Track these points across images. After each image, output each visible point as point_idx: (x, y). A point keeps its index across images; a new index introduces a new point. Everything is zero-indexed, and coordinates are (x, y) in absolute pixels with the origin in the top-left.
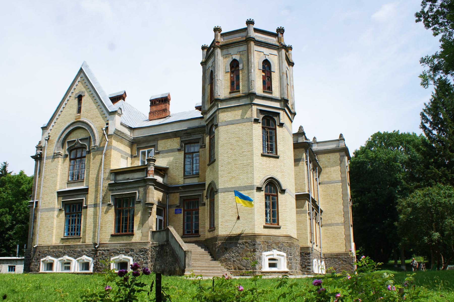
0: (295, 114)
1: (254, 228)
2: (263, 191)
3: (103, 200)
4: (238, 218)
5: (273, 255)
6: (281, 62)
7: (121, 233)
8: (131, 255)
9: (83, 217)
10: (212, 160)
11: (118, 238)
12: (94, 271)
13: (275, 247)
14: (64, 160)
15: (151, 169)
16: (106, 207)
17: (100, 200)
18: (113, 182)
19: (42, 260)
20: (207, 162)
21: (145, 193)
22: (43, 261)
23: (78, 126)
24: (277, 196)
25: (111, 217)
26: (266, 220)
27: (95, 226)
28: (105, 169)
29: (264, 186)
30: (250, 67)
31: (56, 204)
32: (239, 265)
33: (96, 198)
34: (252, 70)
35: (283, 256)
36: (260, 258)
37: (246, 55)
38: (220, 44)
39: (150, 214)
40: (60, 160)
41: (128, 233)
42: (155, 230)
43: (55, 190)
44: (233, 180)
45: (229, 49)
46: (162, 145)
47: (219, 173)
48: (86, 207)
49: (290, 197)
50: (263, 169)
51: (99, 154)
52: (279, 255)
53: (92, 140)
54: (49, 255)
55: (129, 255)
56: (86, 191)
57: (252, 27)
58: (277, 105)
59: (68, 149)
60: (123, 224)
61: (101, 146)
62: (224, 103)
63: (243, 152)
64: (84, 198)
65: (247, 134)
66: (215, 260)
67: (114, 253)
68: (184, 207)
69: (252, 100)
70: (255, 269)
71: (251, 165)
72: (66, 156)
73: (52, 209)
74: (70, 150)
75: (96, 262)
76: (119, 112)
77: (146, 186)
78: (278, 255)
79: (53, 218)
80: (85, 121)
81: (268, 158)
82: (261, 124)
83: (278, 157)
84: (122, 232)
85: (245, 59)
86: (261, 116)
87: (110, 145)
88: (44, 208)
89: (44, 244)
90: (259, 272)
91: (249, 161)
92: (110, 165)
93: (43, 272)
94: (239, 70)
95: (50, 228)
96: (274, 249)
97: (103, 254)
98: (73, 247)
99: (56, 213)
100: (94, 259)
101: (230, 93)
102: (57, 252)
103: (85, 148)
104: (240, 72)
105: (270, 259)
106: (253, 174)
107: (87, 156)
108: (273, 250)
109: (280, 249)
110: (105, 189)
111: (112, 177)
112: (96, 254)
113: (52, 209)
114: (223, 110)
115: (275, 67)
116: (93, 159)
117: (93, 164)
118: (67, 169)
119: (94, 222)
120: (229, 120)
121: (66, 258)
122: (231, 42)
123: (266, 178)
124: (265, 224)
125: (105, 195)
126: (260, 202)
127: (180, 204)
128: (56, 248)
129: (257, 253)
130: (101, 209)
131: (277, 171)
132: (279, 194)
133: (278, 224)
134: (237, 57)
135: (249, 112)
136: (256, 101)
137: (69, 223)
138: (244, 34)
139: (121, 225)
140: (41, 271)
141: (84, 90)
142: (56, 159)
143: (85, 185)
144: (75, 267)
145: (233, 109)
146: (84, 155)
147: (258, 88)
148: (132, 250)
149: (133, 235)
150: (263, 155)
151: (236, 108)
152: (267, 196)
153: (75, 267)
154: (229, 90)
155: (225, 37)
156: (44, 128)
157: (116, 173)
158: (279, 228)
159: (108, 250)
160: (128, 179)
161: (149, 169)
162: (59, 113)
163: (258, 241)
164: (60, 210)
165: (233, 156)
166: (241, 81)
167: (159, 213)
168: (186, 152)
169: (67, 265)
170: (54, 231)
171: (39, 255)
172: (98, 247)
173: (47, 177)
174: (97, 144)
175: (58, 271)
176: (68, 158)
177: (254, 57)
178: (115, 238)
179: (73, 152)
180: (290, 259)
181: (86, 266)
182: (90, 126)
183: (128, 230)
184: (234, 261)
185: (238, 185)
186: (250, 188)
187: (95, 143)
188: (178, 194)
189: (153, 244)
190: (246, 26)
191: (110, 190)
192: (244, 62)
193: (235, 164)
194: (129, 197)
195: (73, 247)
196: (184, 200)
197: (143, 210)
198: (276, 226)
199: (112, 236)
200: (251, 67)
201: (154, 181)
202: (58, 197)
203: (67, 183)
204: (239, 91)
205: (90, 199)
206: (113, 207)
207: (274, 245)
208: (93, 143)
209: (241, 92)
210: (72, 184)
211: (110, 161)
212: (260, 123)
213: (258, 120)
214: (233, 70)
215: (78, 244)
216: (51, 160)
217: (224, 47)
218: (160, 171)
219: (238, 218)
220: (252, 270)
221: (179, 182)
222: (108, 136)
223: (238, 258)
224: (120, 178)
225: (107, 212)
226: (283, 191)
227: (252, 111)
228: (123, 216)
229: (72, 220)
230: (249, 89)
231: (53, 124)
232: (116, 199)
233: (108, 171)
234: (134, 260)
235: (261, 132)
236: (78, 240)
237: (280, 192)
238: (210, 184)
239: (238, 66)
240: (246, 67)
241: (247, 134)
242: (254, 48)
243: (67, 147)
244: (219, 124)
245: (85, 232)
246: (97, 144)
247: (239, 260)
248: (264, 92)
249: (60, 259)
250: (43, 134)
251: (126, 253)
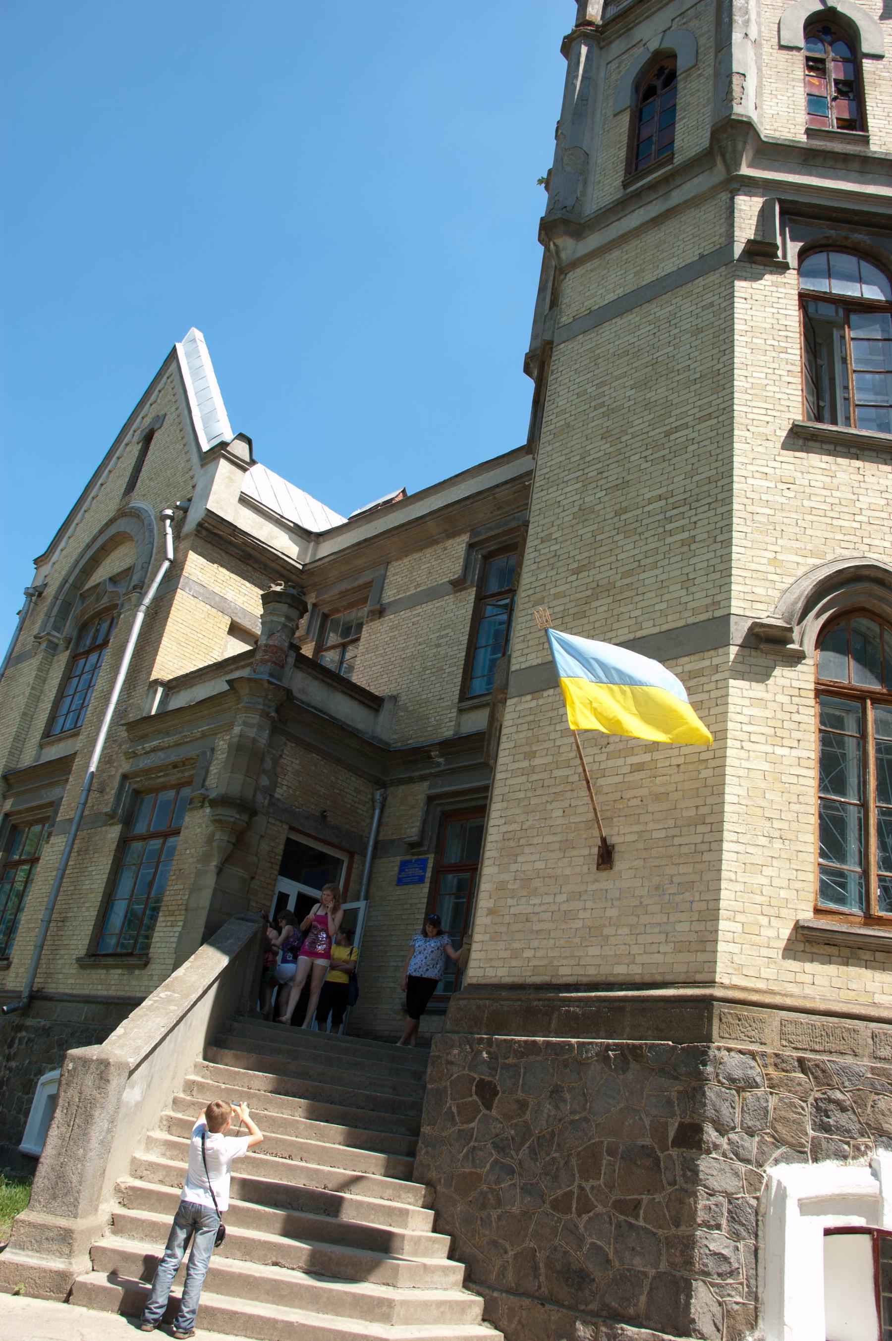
26: (832, 886)
29: (813, 625)
63: (667, 435)
65: (699, 330)
68: (440, 850)
120: (611, 297)
124: (806, 915)
126: (777, 739)
127: (423, 832)
163: (728, 1052)
188: (426, 784)
196: (447, 817)
241: (699, 330)
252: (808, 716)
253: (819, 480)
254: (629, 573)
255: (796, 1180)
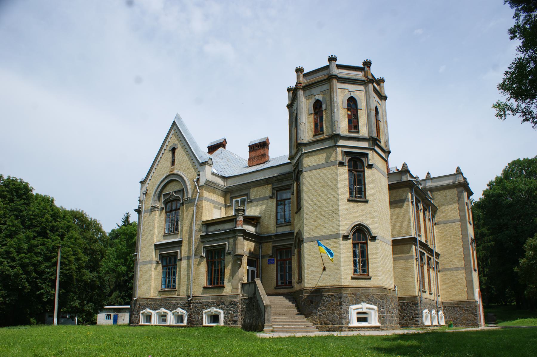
0: (389, 152)
1: (340, 280)
2: (350, 239)
3: (195, 252)
4: (324, 269)
5: (362, 308)
6: (368, 98)
7: (213, 286)
8: (222, 308)
9: (178, 269)
10: (299, 208)
11: (210, 290)
12: (188, 323)
13: (364, 300)
14: (161, 213)
15: (240, 219)
16: (199, 259)
17: (193, 252)
18: (205, 234)
19: (141, 312)
20: (296, 210)
21: (235, 244)
22: (142, 313)
23: (172, 179)
24: (367, 244)
25: (203, 269)
26: (355, 271)
27: (189, 279)
28: (197, 220)
29: (352, 234)
30: (333, 106)
31: (154, 257)
32: (325, 320)
33: (189, 250)
34: (335, 110)
35: (374, 309)
36: (347, 312)
37: (329, 94)
38: (303, 85)
39: (240, 265)
40: (157, 213)
41: (219, 285)
42: (245, 281)
43: (153, 243)
44: (319, 229)
45: (312, 90)
46: (254, 193)
47: (305, 221)
48: (181, 260)
49: (383, 243)
50: (349, 215)
51: (191, 206)
52: (369, 308)
53: (185, 192)
54: (148, 307)
55: (220, 308)
56: (179, 244)
57: (334, 64)
58: (365, 145)
59: (164, 202)
60: (215, 276)
61: (194, 197)
62: (308, 147)
63: (328, 198)
64: (179, 251)
66: (301, 314)
67: (206, 305)
68: (277, 257)
69: (336, 142)
70: (342, 324)
71: (336, 212)
72: (162, 209)
73: (150, 262)
74: (166, 203)
75: (190, 315)
76: (210, 162)
77: (235, 237)
78: (367, 308)
79: (151, 270)
80: (178, 173)
81: (355, 203)
82: (347, 167)
83: (367, 202)
84: (214, 284)
85: (328, 99)
86: (347, 159)
87: (201, 195)
88: (143, 261)
89: (143, 296)
90: (345, 327)
91: (334, 208)
92: (201, 216)
93: (143, 324)
94: (322, 111)
95: (149, 280)
96: (363, 302)
97: (196, 307)
98: (168, 300)
99: (154, 265)
100: (187, 312)
101: (314, 136)
102: (154, 304)
103: (179, 200)
104: (324, 113)
105: (358, 313)
106: (339, 221)
107: (181, 207)
108: (362, 303)
109: (370, 302)
110: (197, 241)
111: (204, 229)
112: (190, 306)
113: (150, 262)
114: (307, 154)
115: (362, 104)
116: (186, 211)
117: (186, 216)
118: (163, 222)
119: (187, 274)
121: (163, 310)
122: (313, 82)
123: (353, 225)
124: (352, 275)
125: (197, 247)
126: (347, 252)
127: (273, 254)
128: (154, 301)
129: (344, 307)
130: (194, 261)
131: (366, 217)
132: (369, 242)
133: (368, 275)
134: (320, 97)
135: (333, 155)
136: (341, 143)
137: (166, 276)
138: (326, 72)
139: (213, 277)
140: (140, 323)
141: (177, 142)
142: (153, 213)
143: (179, 237)
144: (171, 320)
145: (317, 152)
146: (178, 208)
147: (343, 127)
148: (223, 303)
149: (223, 287)
150: (349, 201)
151: (321, 152)
152: (354, 245)
153: (171, 320)
154: (312, 133)
155: (308, 77)
156: (142, 183)
157: (208, 224)
158: (370, 279)
159: (201, 303)
160: (219, 230)
161: (238, 219)
162: (155, 166)
163: (345, 293)
164: (158, 262)
165: (318, 203)
166: (324, 122)
167: (250, 263)
168: (279, 199)
169: (163, 318)
170: (153, 284)
171: (139, 307)
172: (191, 300)
173: (145, 230)
174: (190, 196)
175: (155, 324)
176: (164, 211)
177: (337, 95)
178: (207, 291)
179: (169, 204)
180: (383, 313)
181: (180, 318)
182: (183, 178)
183: (219, 282)
184: (320, 315)
185: (323, 234)
186: (335, 236)
187: (187, 195)
189: (243, 296)
190: (328, 63)
191: (202, 242)
192: (328, 102)
193: (321, 212)
194: (220, 249)
195: (168, 300)
196: (277, 250)
197: (233, 262)
198: (366, 276)
199: (204, 288)
200: (334, 106)
201: (244, 232)
202: (156, 249)
203: (164, 236)
204: (323, 134)
205: (184, 252)
206: (205, 259)
207: (363, 297)
208: (185, 195)
209: (325, 134)
210: (168, 237)
211: (202, 212)
212: (345, 165)
213: (343, 163)
214: (317, 111)
215: (174, 296)
216: (148, 213)
217: (306, 88)
218: (249, 220)
219: (324, 269)
220: (337, 326)
221: (271, 231)
222: (199, 187)
223: (324, 312)
224: (212, 229)
225: (199, 264)
226: (374, 239)
227: (336, 153)
228: (215, 268)
229: (169, 272)
230: (333, 131)
231: (150, 178)
232: (208, 251)
233: (200, 223)
234: (224, 313)
235: (347, 175)
236: (174, 293)
237: (370, 240)
238: (297, 233)
239: (321, 106)
240: (329, 108)
241: (331, 179)
242: (338, 86)
243: (163, 200)
244: (304, 170)
245: (179, 284)
246: (190, 196)
247: (325, 314)
248: (349, 132)
249: (157, 311)
250: (141, 189)
251: (217, 306)
252: (351, 247)
253: (352, 208)
254: (323, 224)
255: (353, 307)
